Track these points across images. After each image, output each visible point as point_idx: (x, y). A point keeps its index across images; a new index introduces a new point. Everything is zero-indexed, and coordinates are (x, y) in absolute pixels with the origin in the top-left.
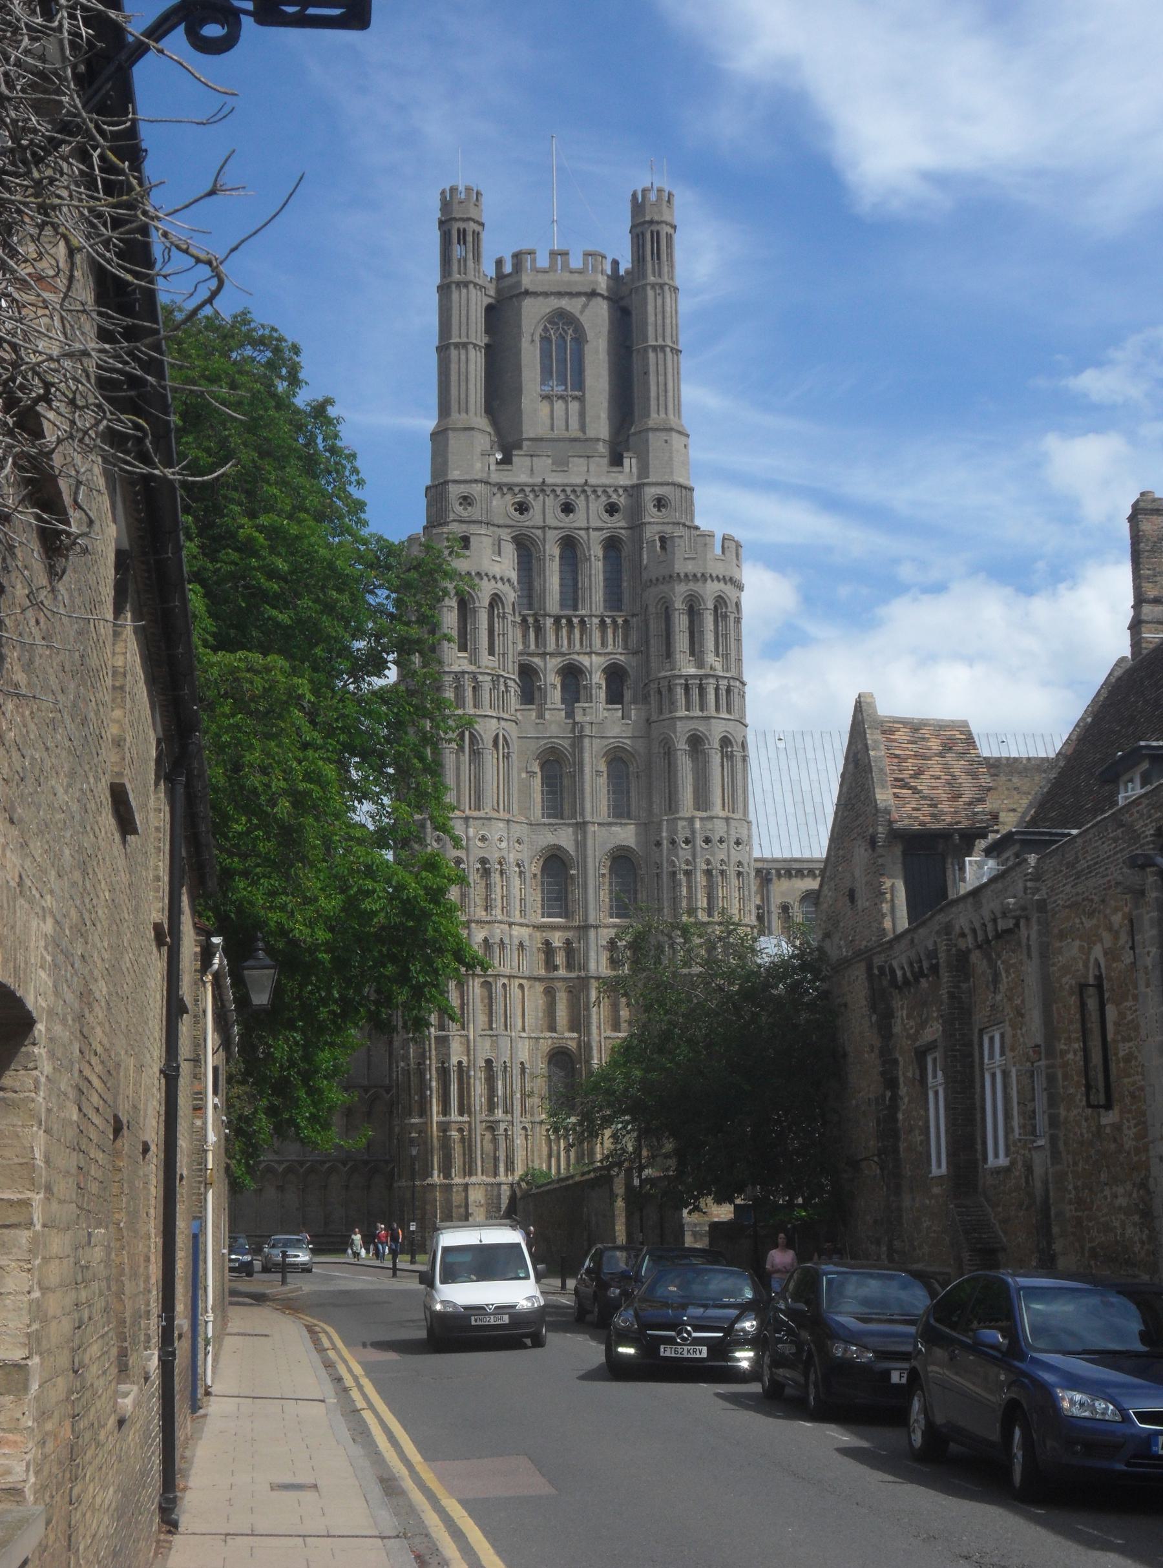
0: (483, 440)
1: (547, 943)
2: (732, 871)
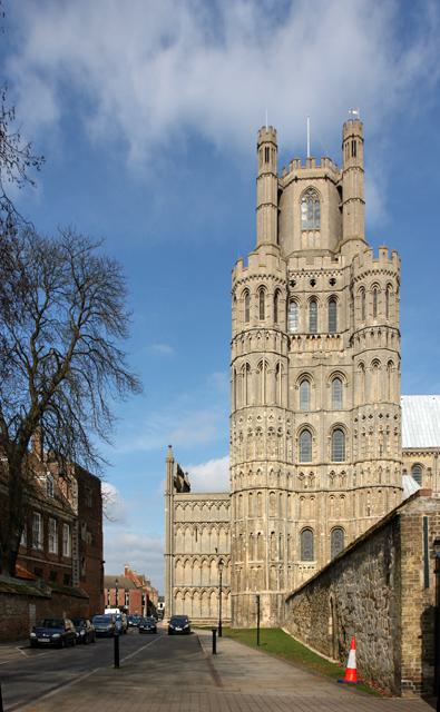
1: (302, 474)
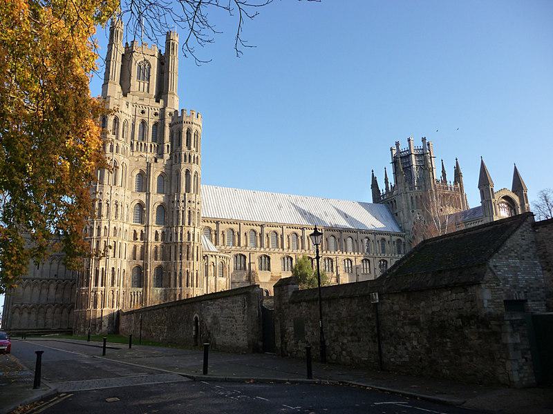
0: (119, 89)
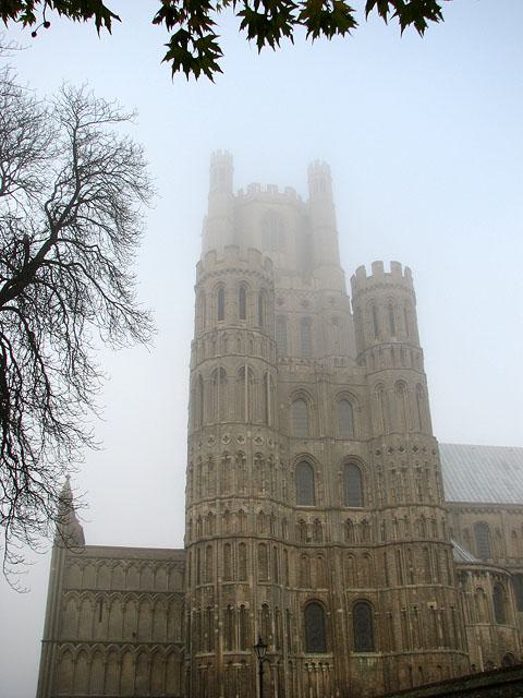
1: (302, 522)
2: (432, 471)
